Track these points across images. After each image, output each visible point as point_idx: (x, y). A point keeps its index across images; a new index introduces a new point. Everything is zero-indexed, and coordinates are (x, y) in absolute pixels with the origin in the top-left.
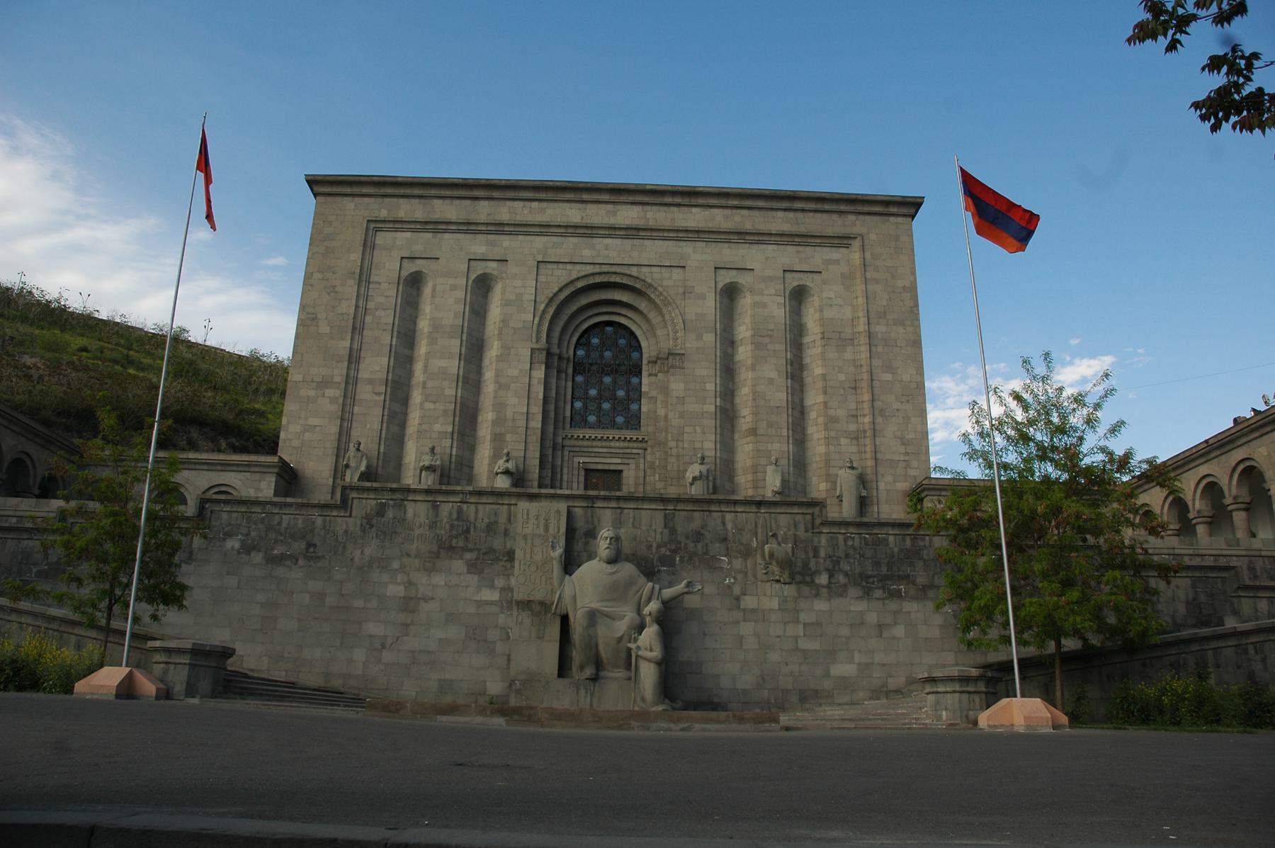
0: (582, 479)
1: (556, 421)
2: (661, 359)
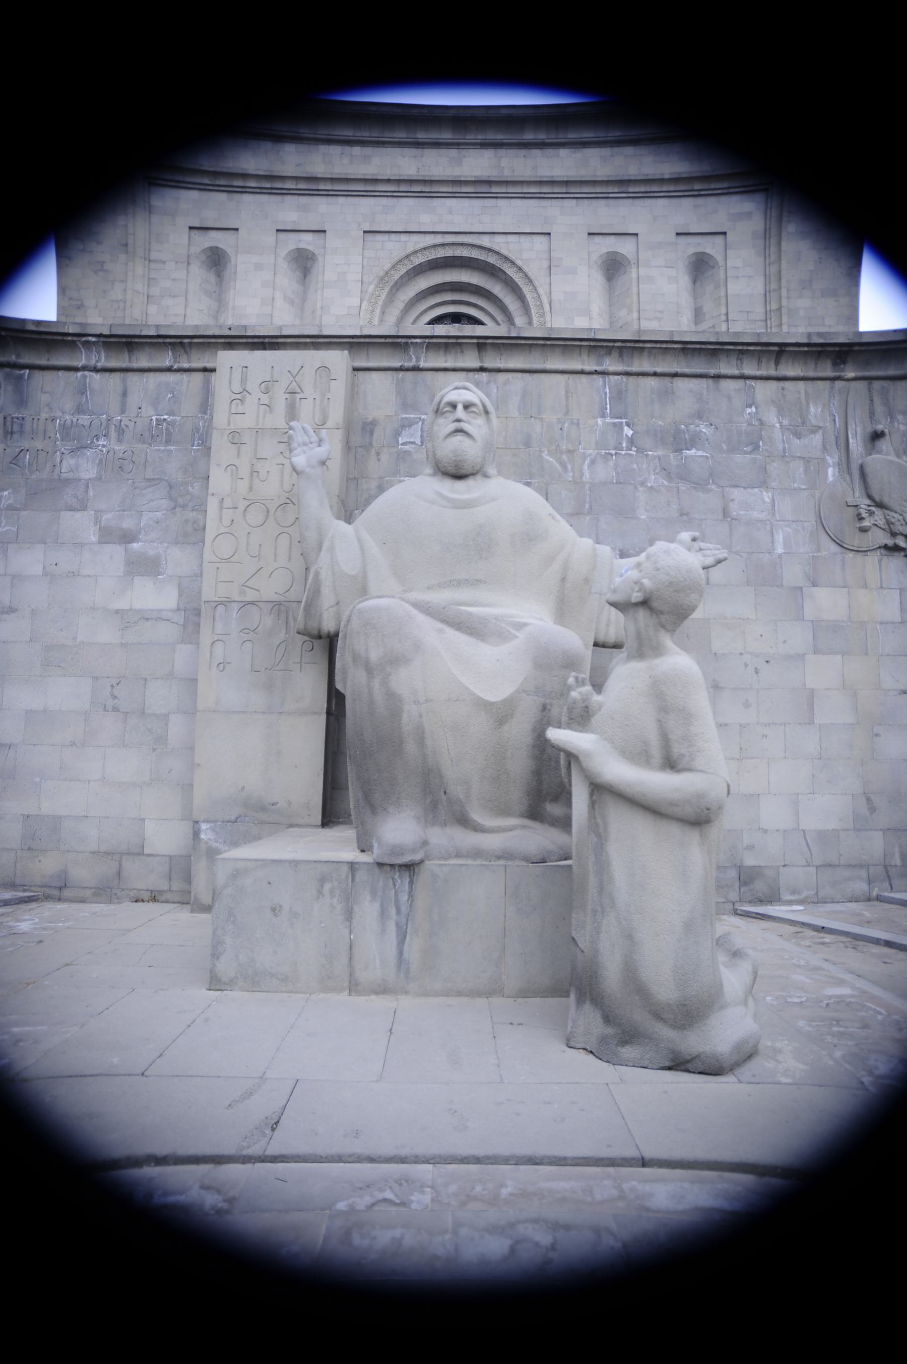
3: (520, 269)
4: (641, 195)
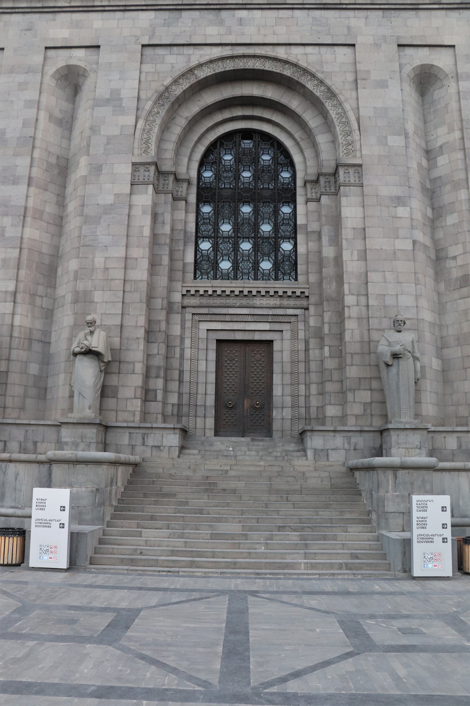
0: (212, 355)
1: (172, 270)
2: (325, 175)
3: (321, 82)
4: (456, 6)
